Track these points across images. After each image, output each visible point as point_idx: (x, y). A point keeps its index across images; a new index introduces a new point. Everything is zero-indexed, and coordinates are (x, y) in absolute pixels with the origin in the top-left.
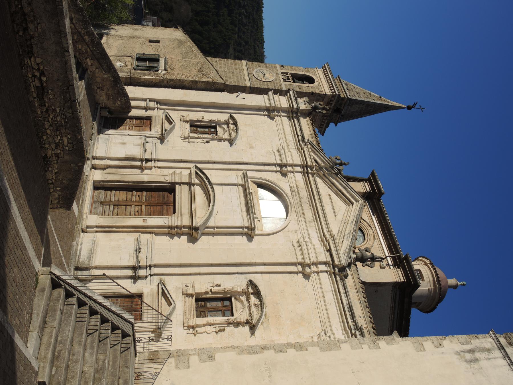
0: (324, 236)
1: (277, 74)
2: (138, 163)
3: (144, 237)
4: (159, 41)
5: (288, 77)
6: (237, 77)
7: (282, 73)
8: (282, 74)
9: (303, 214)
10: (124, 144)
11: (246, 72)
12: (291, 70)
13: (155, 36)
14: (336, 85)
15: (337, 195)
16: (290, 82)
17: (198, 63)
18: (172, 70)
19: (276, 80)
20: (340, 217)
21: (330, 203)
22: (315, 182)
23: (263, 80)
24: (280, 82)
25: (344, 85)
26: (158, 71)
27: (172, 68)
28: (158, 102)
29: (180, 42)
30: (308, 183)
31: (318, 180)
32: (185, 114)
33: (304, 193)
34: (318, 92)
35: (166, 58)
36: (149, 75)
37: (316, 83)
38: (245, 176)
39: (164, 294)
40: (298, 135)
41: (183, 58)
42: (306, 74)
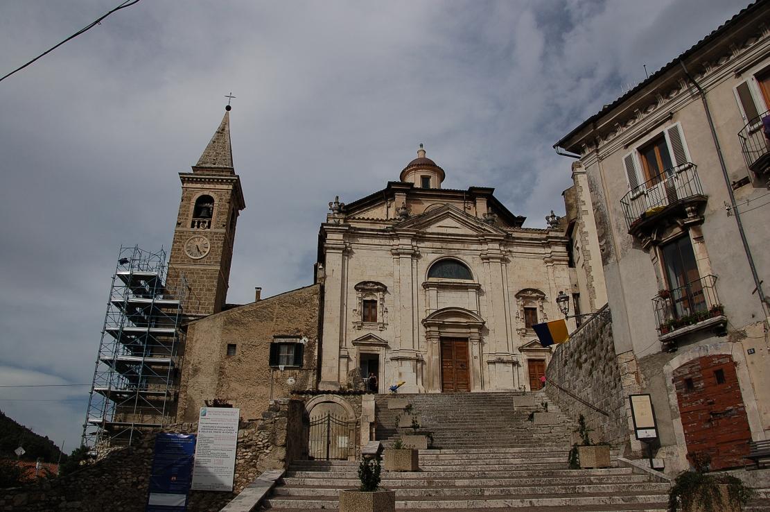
0: (479, 240)
1: (194, 233)
2: (419, 365)
3: (485, 359)
4: (235, 345)
5: (199, 223)
6: (202, 278)
7: (193, 226)
8: (196, 227)
9: (458, 249)
10: (400, 374)
11: (191, 267)
12: (187, 216)
13: (218, 349)
14: (220, 176)
15: (438, 221)
16: (210, 223)
17: (283, 306)
18: (299, 331)
19: (206, 237)
20: (458, 225)
21: (446, 228)
22: (430, 234)
23: (208, 251)
24: (211, 233)
25: (207, 165)
26: (304, 346)
27: (296, 331)
28: (340, 348)
29: (231, 323)
30: (429, 240)
31: (429, 230)
32: (350, 326)
33: (438, 245)
34: (228, 197)
35: (275, 337)
36: (312, 352)
37: (212, 194)
38: (426, 286)
39: (529, 346)
40: (377, 234)
41: (272, 320)
42: (194, 200)
